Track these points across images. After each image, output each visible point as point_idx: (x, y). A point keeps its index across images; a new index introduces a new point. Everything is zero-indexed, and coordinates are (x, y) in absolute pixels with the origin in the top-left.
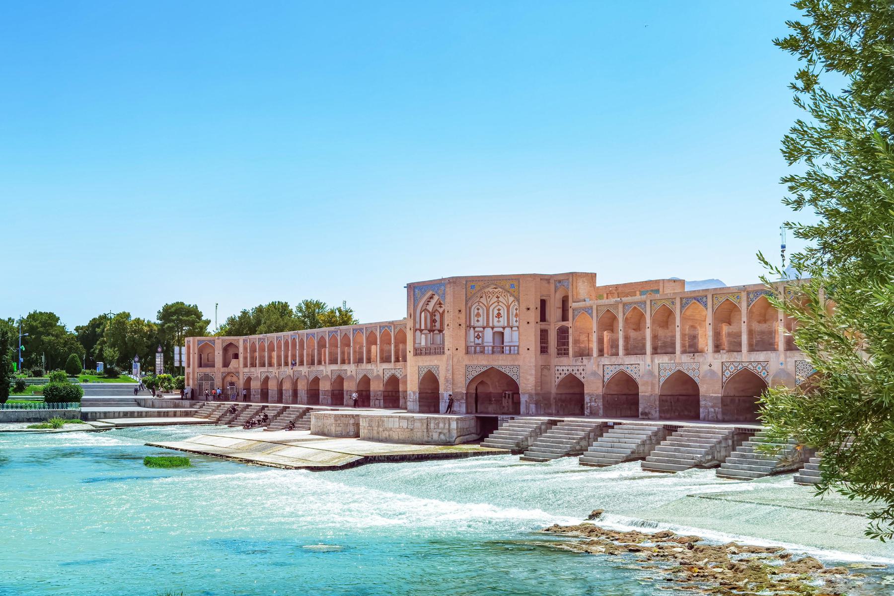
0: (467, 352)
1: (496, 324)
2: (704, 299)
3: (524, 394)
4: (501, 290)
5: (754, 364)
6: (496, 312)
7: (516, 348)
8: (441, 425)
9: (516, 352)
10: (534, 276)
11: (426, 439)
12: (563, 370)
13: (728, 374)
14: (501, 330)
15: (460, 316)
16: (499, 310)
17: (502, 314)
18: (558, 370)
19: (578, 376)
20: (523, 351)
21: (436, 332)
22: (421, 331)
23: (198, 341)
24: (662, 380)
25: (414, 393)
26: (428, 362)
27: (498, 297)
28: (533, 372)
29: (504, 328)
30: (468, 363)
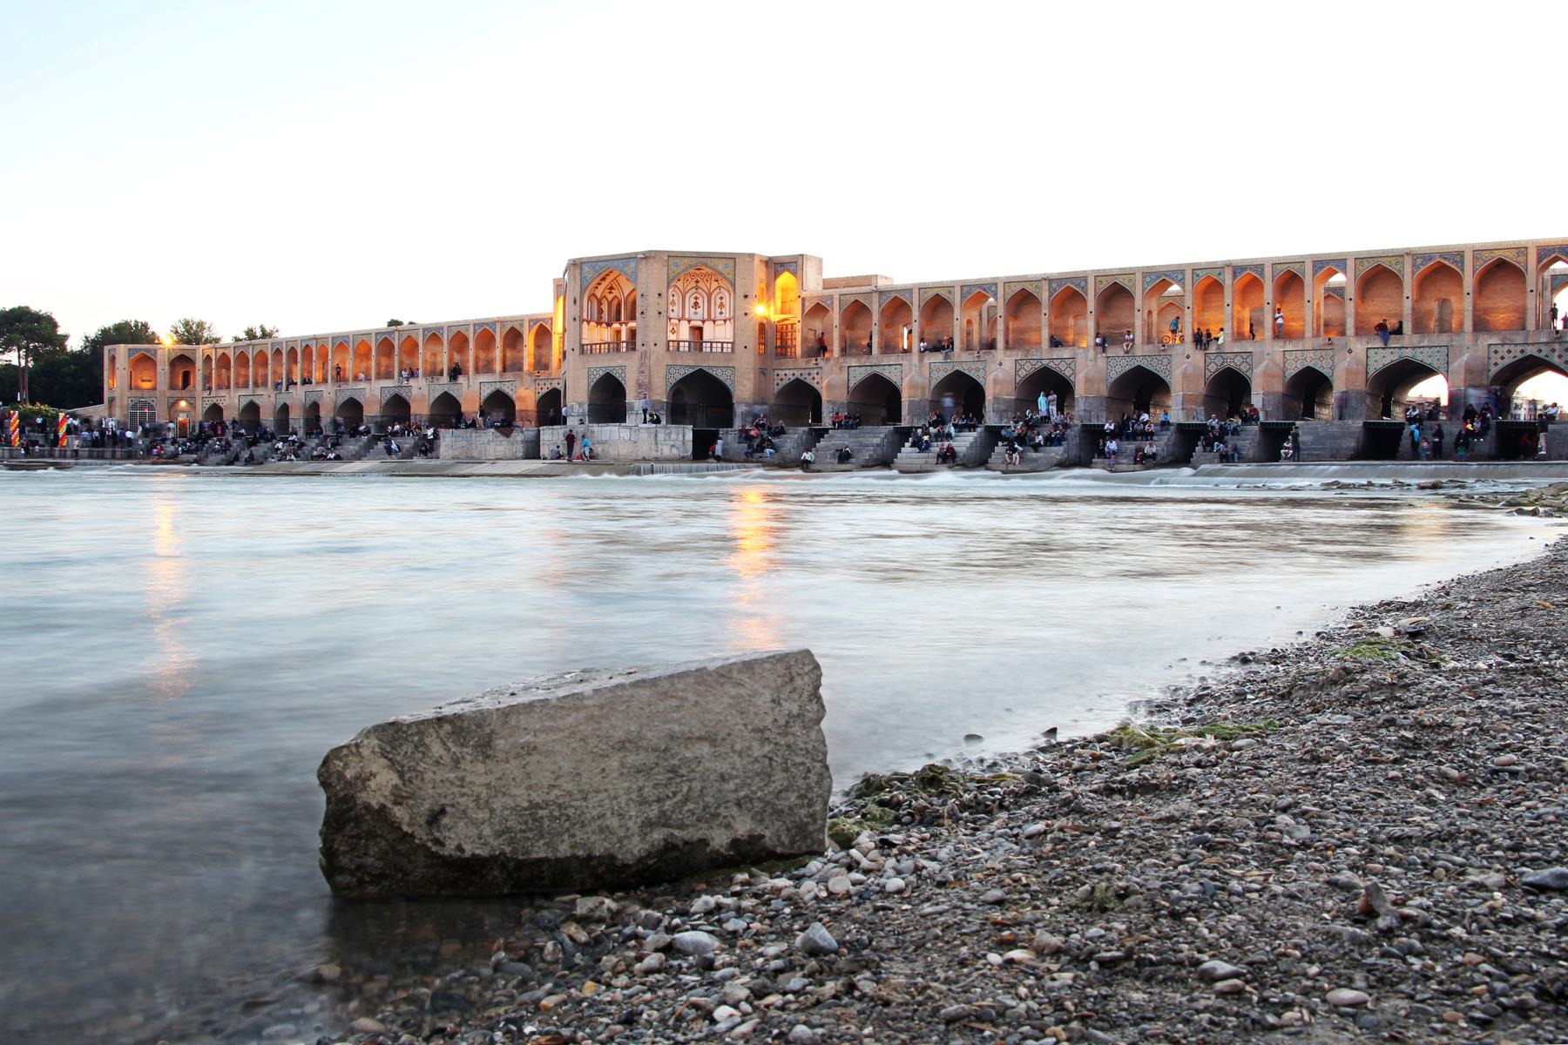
1: (692, 317)
3: (739, 403)
4: (710, 271)
5: (1057, 362)
6: (693, 301)
8: (673, 436)
11: (654, 454)
13: (1023, 373)
14: (700, 324)
15: (660, 301)
19: (809, 381)
20: (739, 348)
22: (588, 322)
24: (934, 382)
25: (580, 405)
27: (697, 282)
28: (751, 376)
29: (703, 322)
30: (670, 363)
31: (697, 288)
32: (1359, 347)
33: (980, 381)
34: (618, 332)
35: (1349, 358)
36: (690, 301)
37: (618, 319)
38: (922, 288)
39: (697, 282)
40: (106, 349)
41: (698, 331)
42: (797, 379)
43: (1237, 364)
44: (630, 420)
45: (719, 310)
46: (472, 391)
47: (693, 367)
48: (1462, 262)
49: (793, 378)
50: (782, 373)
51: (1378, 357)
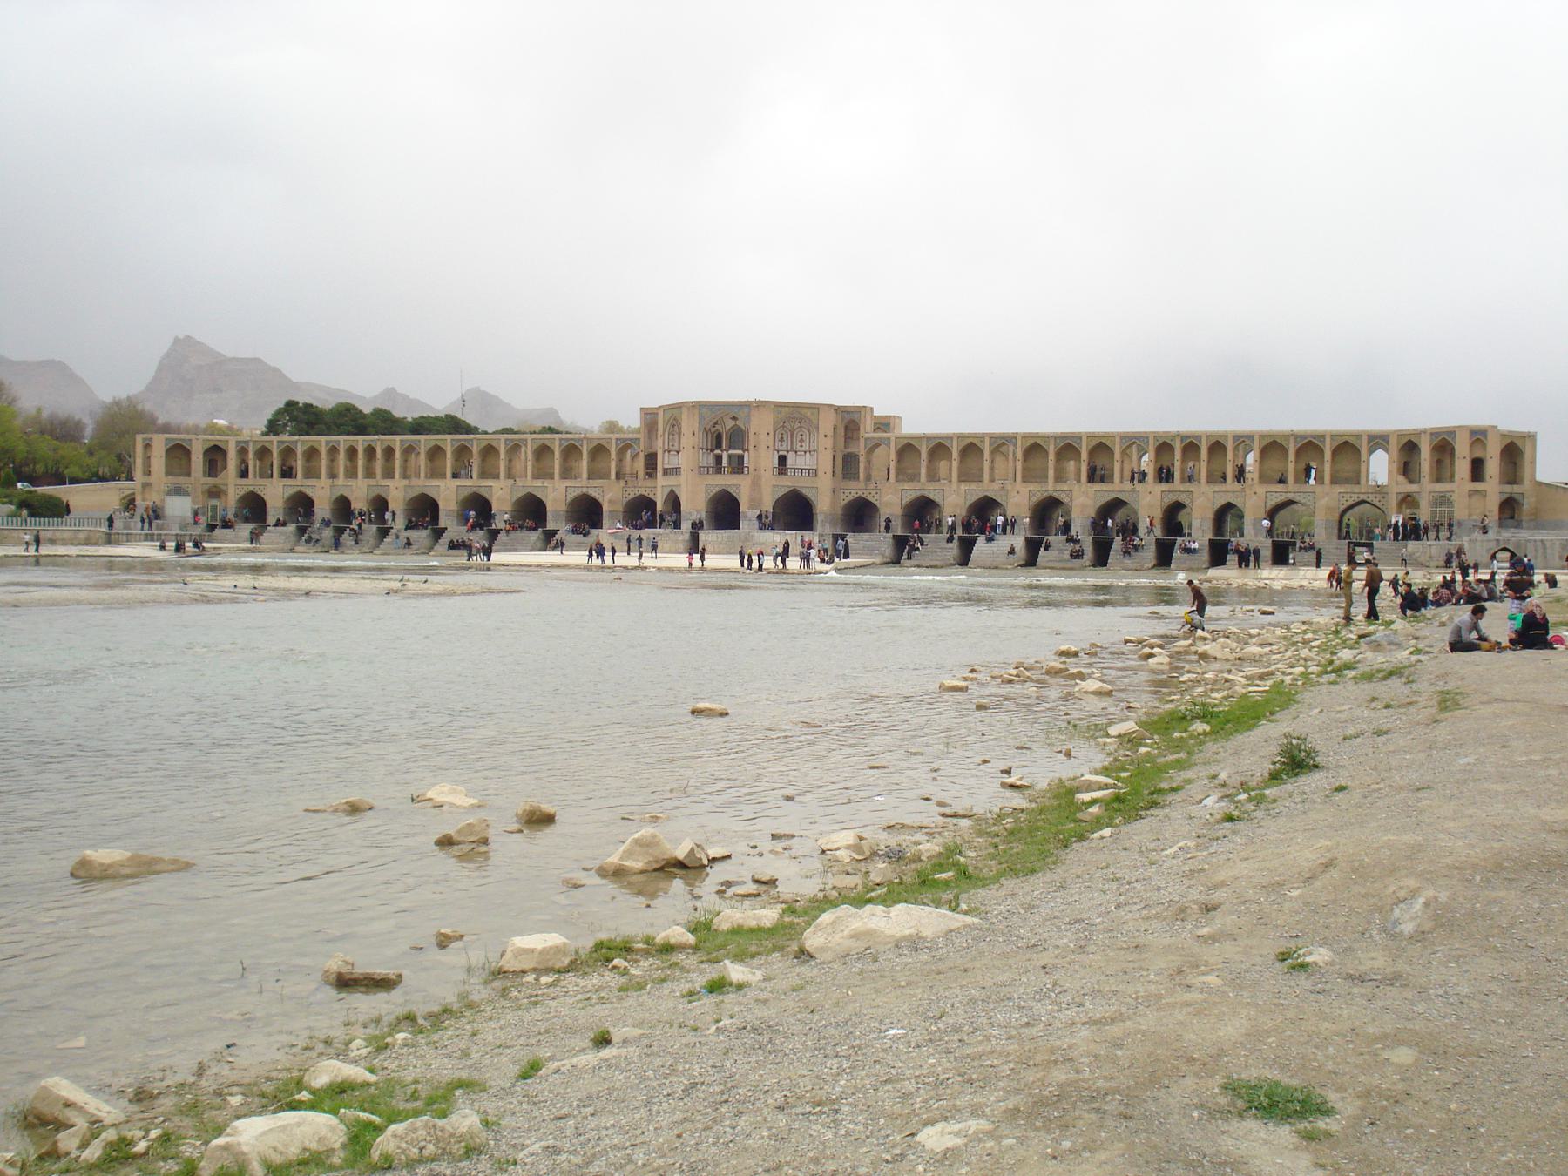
14: (785, 453)
20: (820, 473)
23: (167, 439)
26: (726, 481)
31: (783, 427)
32: (1262, 490)
34: (719, 459)
35: (1255, 498)
36: (797, 437)
37: (719, 445)
38: (961, 437)
40: (139, 438)
41: (782, 459)
46: (557, 495)
47: (788, 487)
48: (1324, 441)
49: (856, 496)
50: (847, 492)
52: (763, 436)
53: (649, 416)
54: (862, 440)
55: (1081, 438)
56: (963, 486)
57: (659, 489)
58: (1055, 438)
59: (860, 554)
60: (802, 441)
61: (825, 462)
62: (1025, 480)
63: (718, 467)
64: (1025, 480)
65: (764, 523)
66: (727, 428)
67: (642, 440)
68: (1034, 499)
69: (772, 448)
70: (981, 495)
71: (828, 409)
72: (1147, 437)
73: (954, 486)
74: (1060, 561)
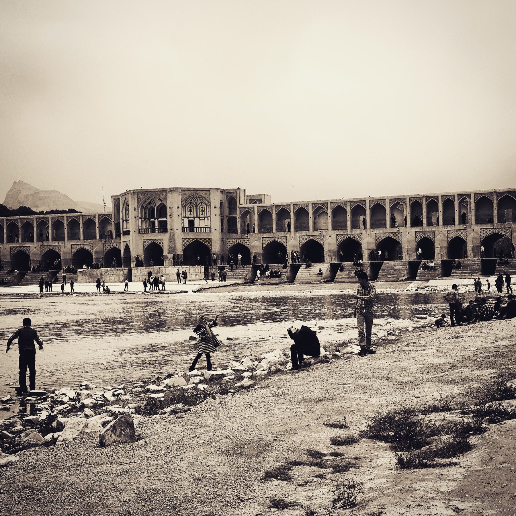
0: (183, 231)
1: (189, 216)
2: (326, 205)
7: (209, 229)
8: (197, 271)
9: (209, 231)
10: (217, 189)
12: (233, 241)
14: (193, 219)
15: (178, 210)
16: (190, 208)
17: (193, 210)
18: (229, 241)
19: (244, 244)
20: (213, 230)
21: (147, 220)
27: (191, 200)
29: (194, 218)
31: (191, 203)
32: (477, 228)
33: (322, 243)
34: (153, 223)
39: (191, 200)
41: (191, 223)
42: (238, 243)
43: (428, 235)
44: (166, 263)
45: (201, 213)
47: (194, 239)
51: (484, 232)
52: (175, 209)
53: (116, 200)
54: (238, 209)
55: (365, 201)
56: (298, 234)
57: (122, 243)
58: (351, 202)
59: (231, 277)
60: (202, 211)
61: (216, 223)
62: (334, 228)
63: (153, 230)
64: (334, 228)
65: (177, 261)
66: (157, 205)
67: (113, 216)
68: (340, 240)
69: (180, 216)
70: (308, 239)
71: (215, 191)
72: (405, 199)
73: (292, 234)
74: (348, 278)
